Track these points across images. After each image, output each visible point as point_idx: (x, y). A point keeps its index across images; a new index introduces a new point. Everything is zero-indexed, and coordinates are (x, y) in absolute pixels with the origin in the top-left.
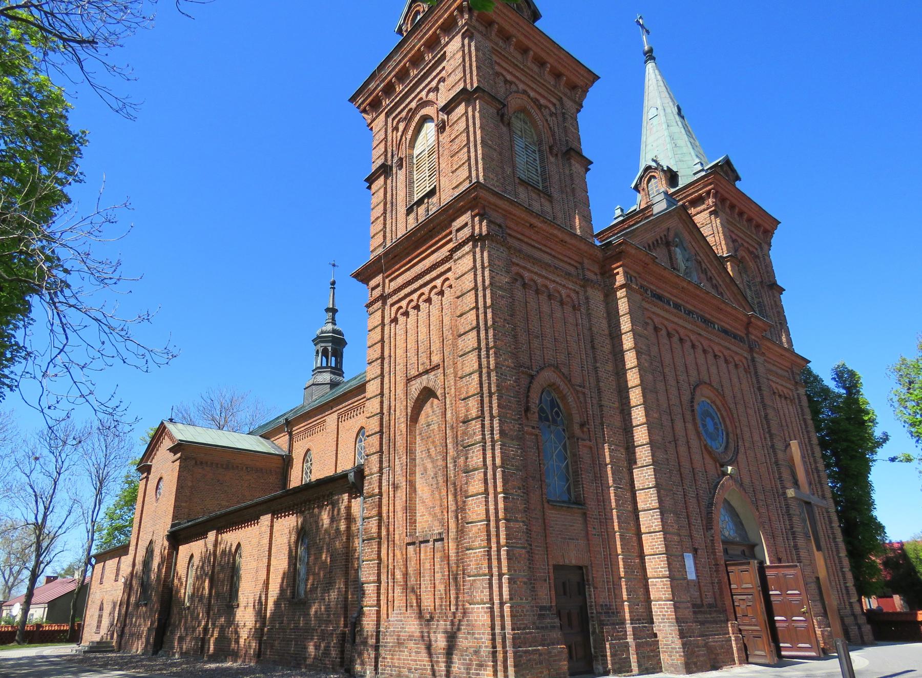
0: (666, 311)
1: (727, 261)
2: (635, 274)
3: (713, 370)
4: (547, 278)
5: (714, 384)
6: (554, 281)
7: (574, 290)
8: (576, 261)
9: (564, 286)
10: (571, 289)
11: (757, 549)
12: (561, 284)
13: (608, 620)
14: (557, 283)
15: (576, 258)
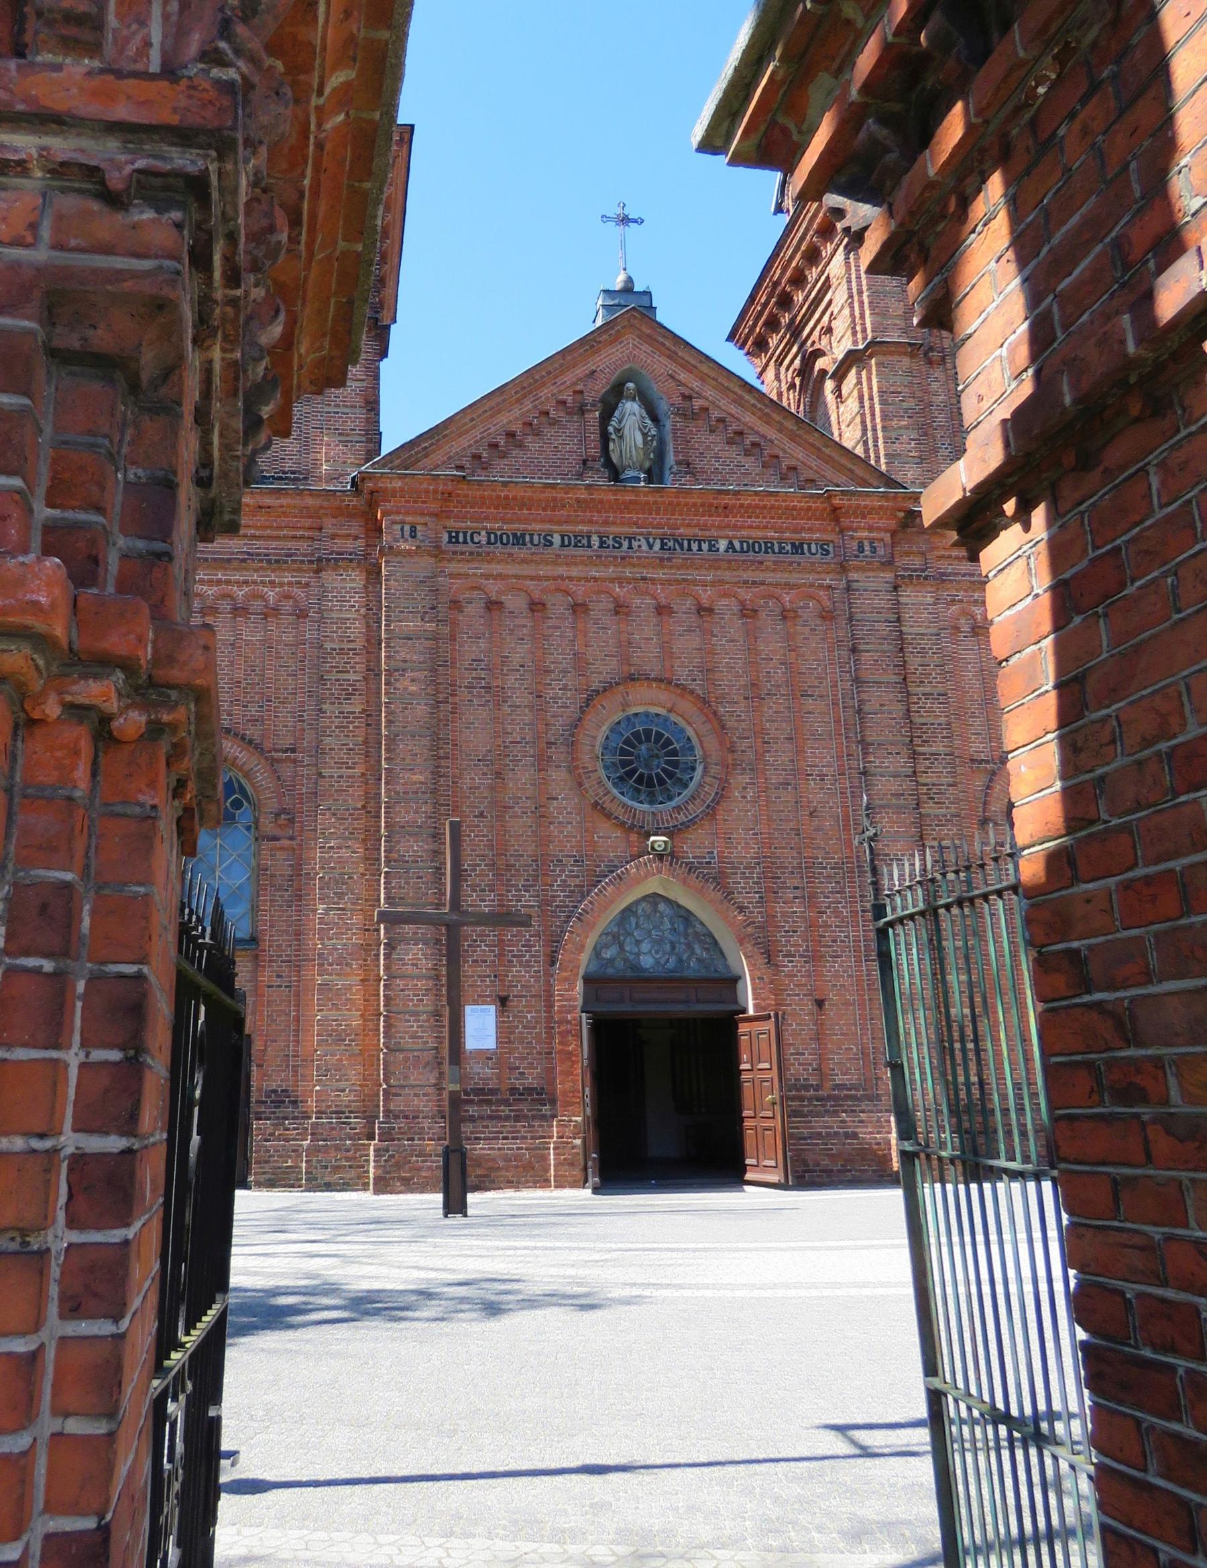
0: (524, 561)
1: (870, 357)
2: (422, 520)
3: (687, 645)
4: (228, 582)
5: (683, 676)
6: (246, 582)
7: (299, 583)
8: (310, 528)
9: (272, 583)
10: (290, 584)
11: (740, 985)
12: (263, 582)
13: (274, 1113)
14: (255, 582)
15: (308, 523)
